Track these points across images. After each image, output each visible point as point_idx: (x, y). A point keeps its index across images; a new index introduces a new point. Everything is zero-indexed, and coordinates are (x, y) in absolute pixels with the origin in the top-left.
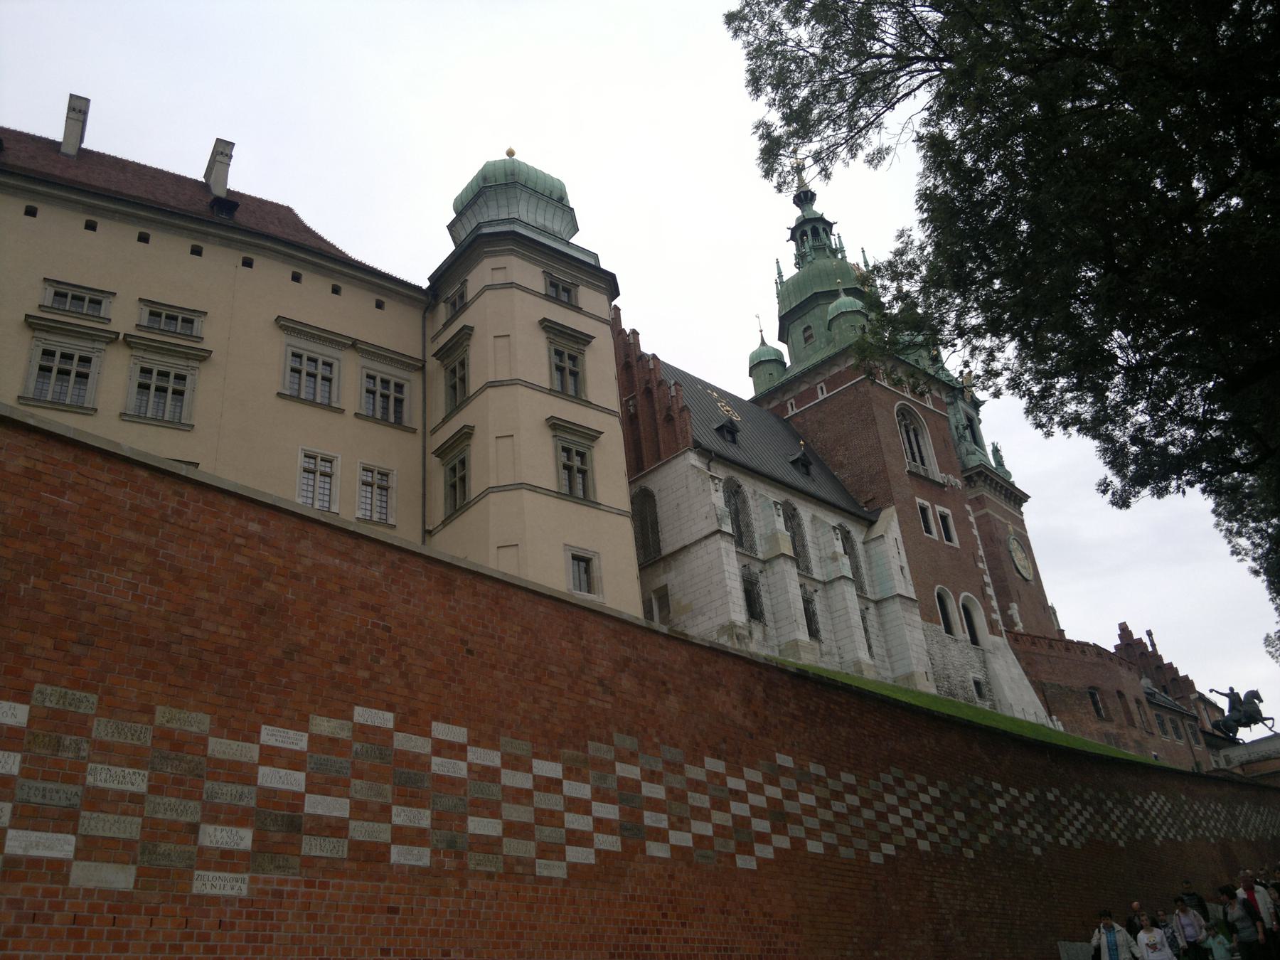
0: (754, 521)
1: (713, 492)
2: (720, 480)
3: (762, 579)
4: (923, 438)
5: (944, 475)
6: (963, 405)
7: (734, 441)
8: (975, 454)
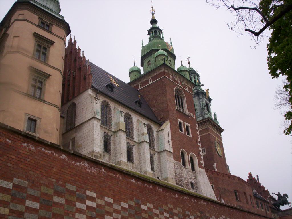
1: (95, 103)
3: (112, 138)
5: (189, 113)
7: (112, 91)
8: (207, 114)
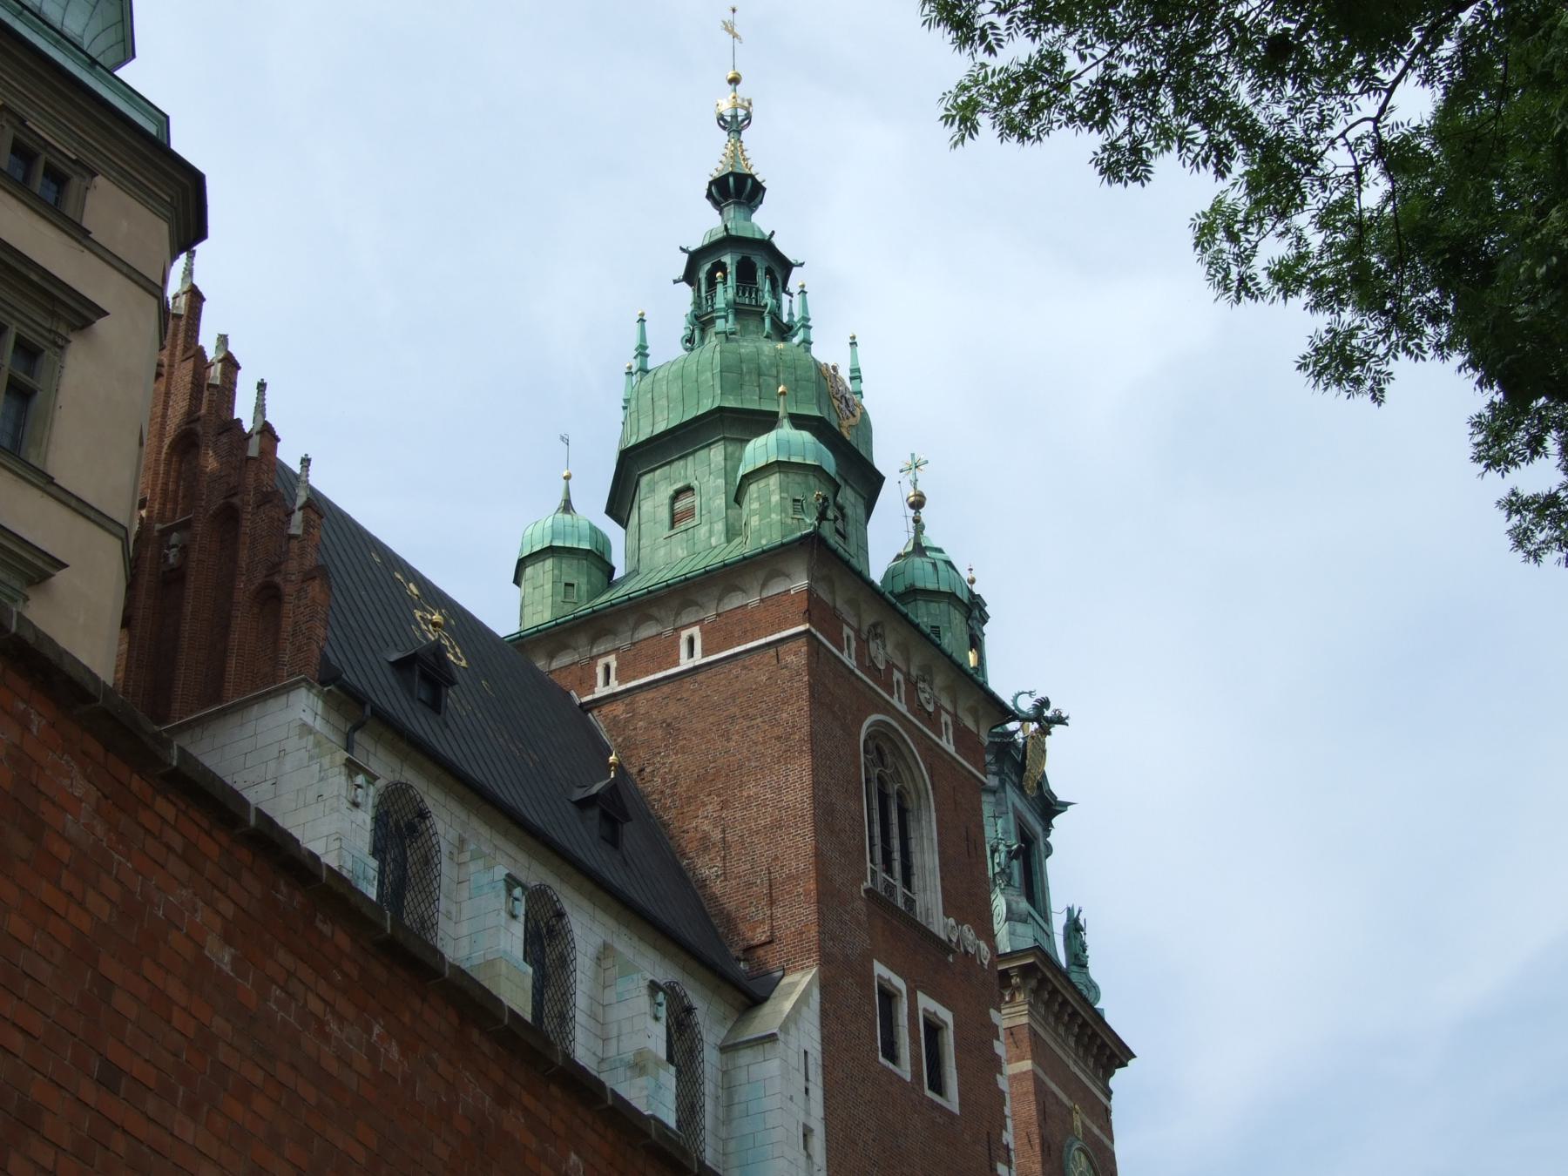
0: (442, 919)
2: (372, 778)
4: (919, 821)
5: (952, 921)
6: (1017, 802)
